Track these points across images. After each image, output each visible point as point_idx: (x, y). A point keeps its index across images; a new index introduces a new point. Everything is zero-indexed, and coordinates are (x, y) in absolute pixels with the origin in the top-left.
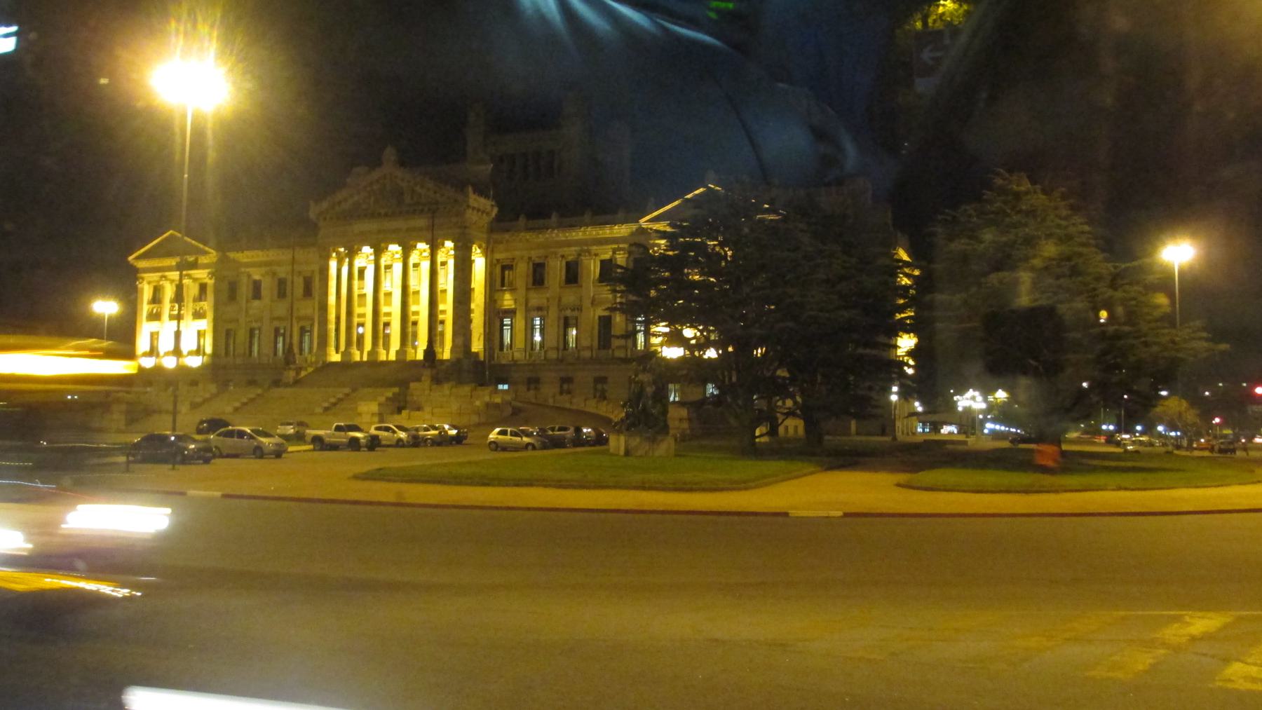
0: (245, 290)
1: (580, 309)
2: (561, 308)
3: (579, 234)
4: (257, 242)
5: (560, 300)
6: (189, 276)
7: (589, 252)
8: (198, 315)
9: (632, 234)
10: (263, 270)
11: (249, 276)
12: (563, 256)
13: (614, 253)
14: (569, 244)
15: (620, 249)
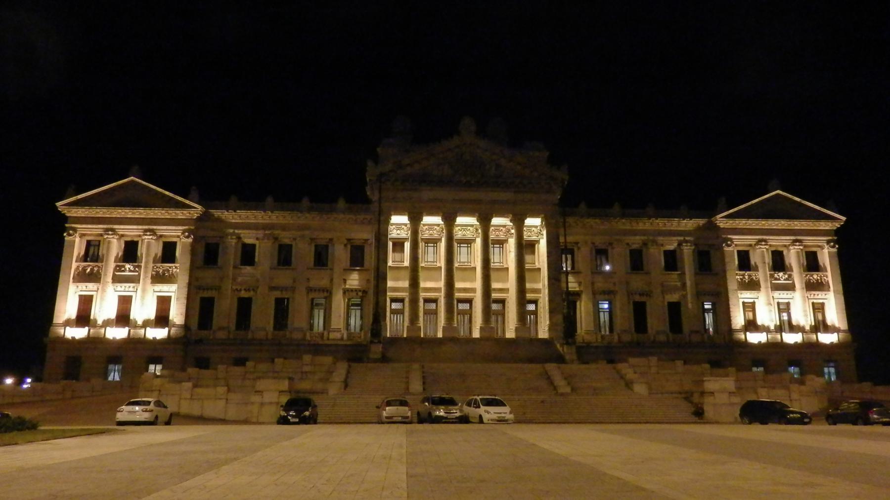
0: (230, 254)
1: (648, 294)
2: (630, 294)
3: (644, 225)
4: (251, 198)
5: (628, 283)
6: (153, 232)
7: (655, 242)
8: (159, 278)
9: (699, 228)
10: (260, 234)
11: (239, 238)
12: (628, 244)
13: (680, 244)
14: (635, 233)
15: (687, 242)
